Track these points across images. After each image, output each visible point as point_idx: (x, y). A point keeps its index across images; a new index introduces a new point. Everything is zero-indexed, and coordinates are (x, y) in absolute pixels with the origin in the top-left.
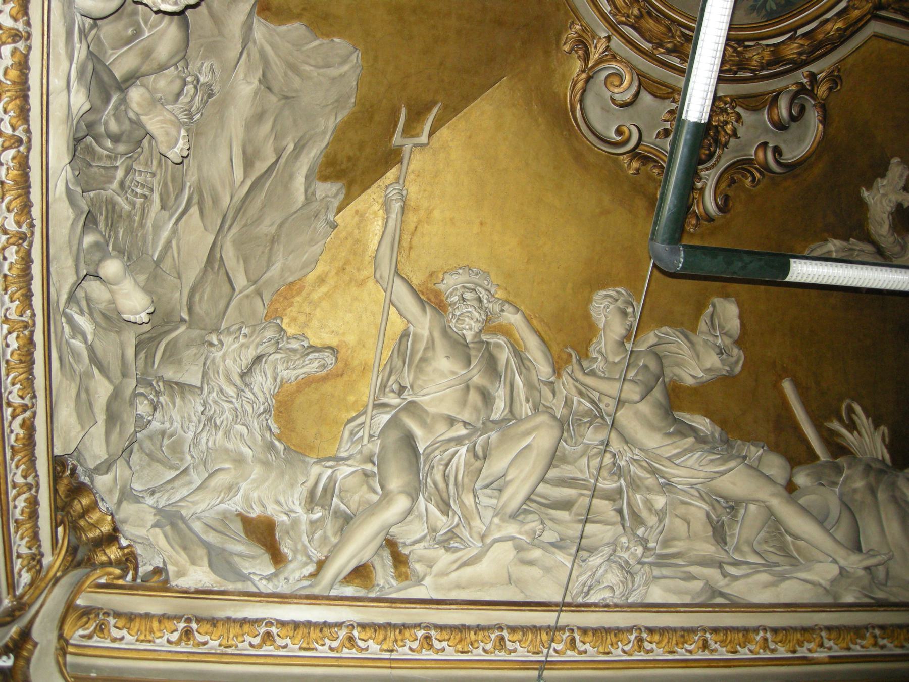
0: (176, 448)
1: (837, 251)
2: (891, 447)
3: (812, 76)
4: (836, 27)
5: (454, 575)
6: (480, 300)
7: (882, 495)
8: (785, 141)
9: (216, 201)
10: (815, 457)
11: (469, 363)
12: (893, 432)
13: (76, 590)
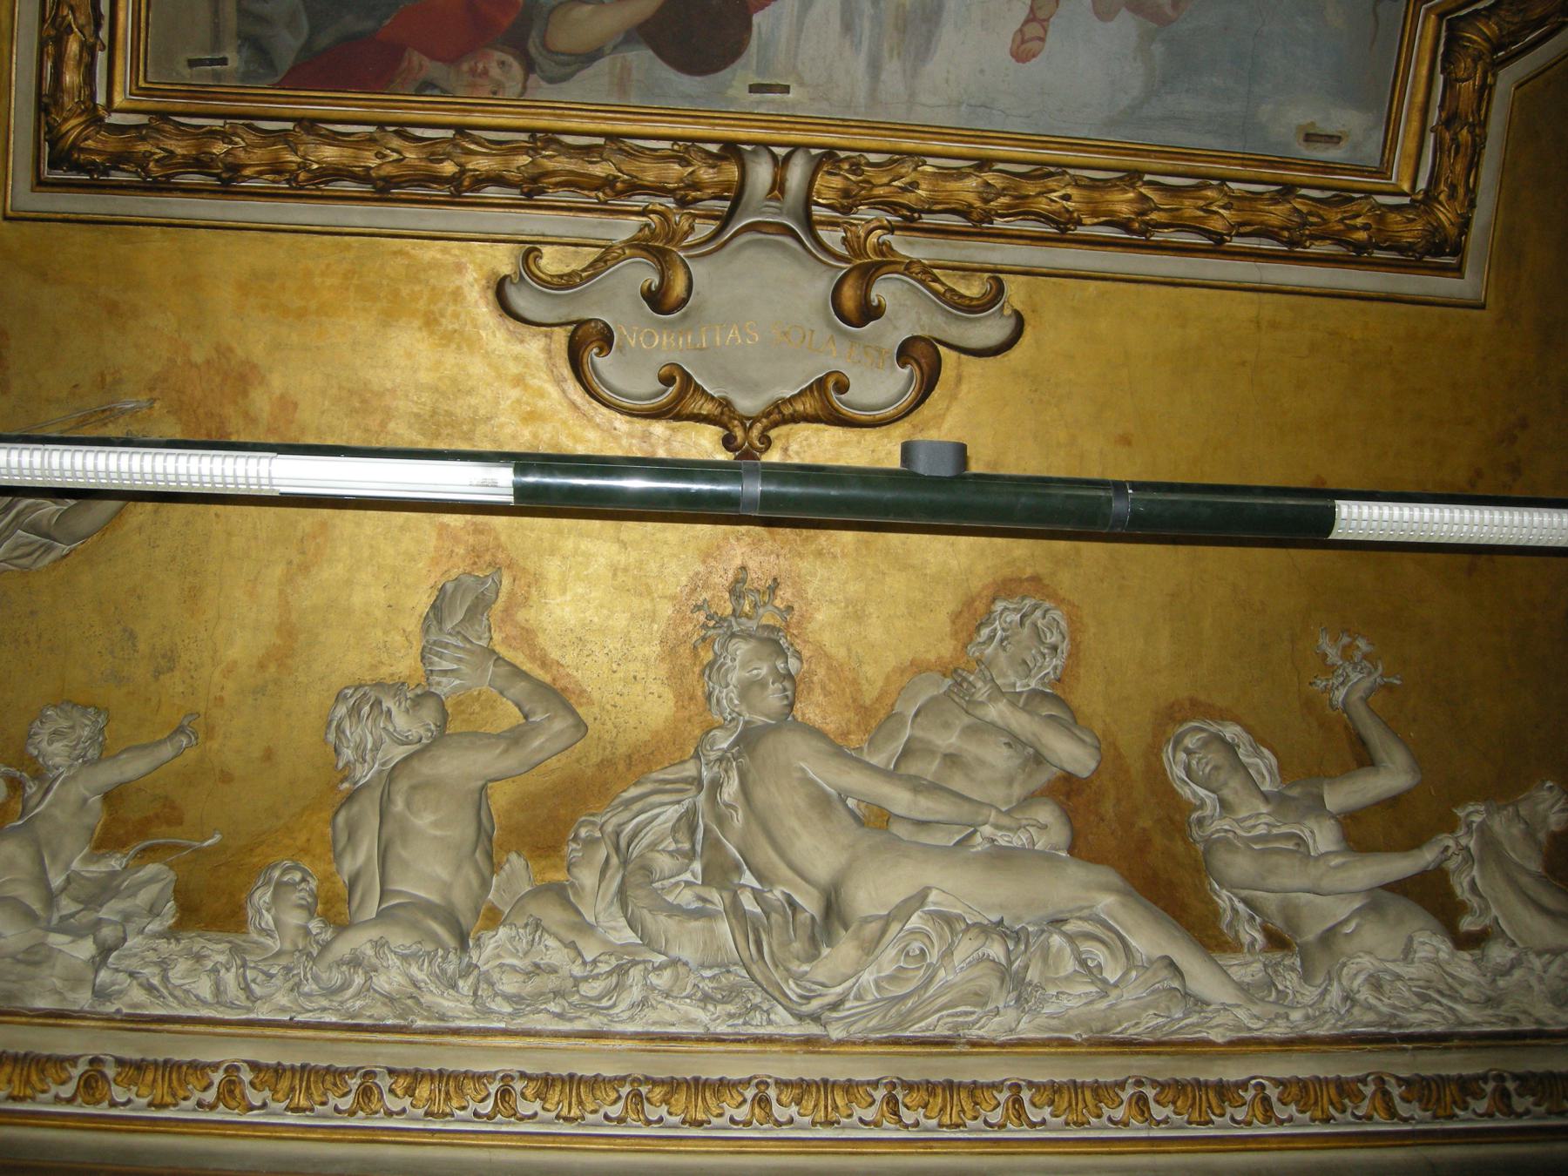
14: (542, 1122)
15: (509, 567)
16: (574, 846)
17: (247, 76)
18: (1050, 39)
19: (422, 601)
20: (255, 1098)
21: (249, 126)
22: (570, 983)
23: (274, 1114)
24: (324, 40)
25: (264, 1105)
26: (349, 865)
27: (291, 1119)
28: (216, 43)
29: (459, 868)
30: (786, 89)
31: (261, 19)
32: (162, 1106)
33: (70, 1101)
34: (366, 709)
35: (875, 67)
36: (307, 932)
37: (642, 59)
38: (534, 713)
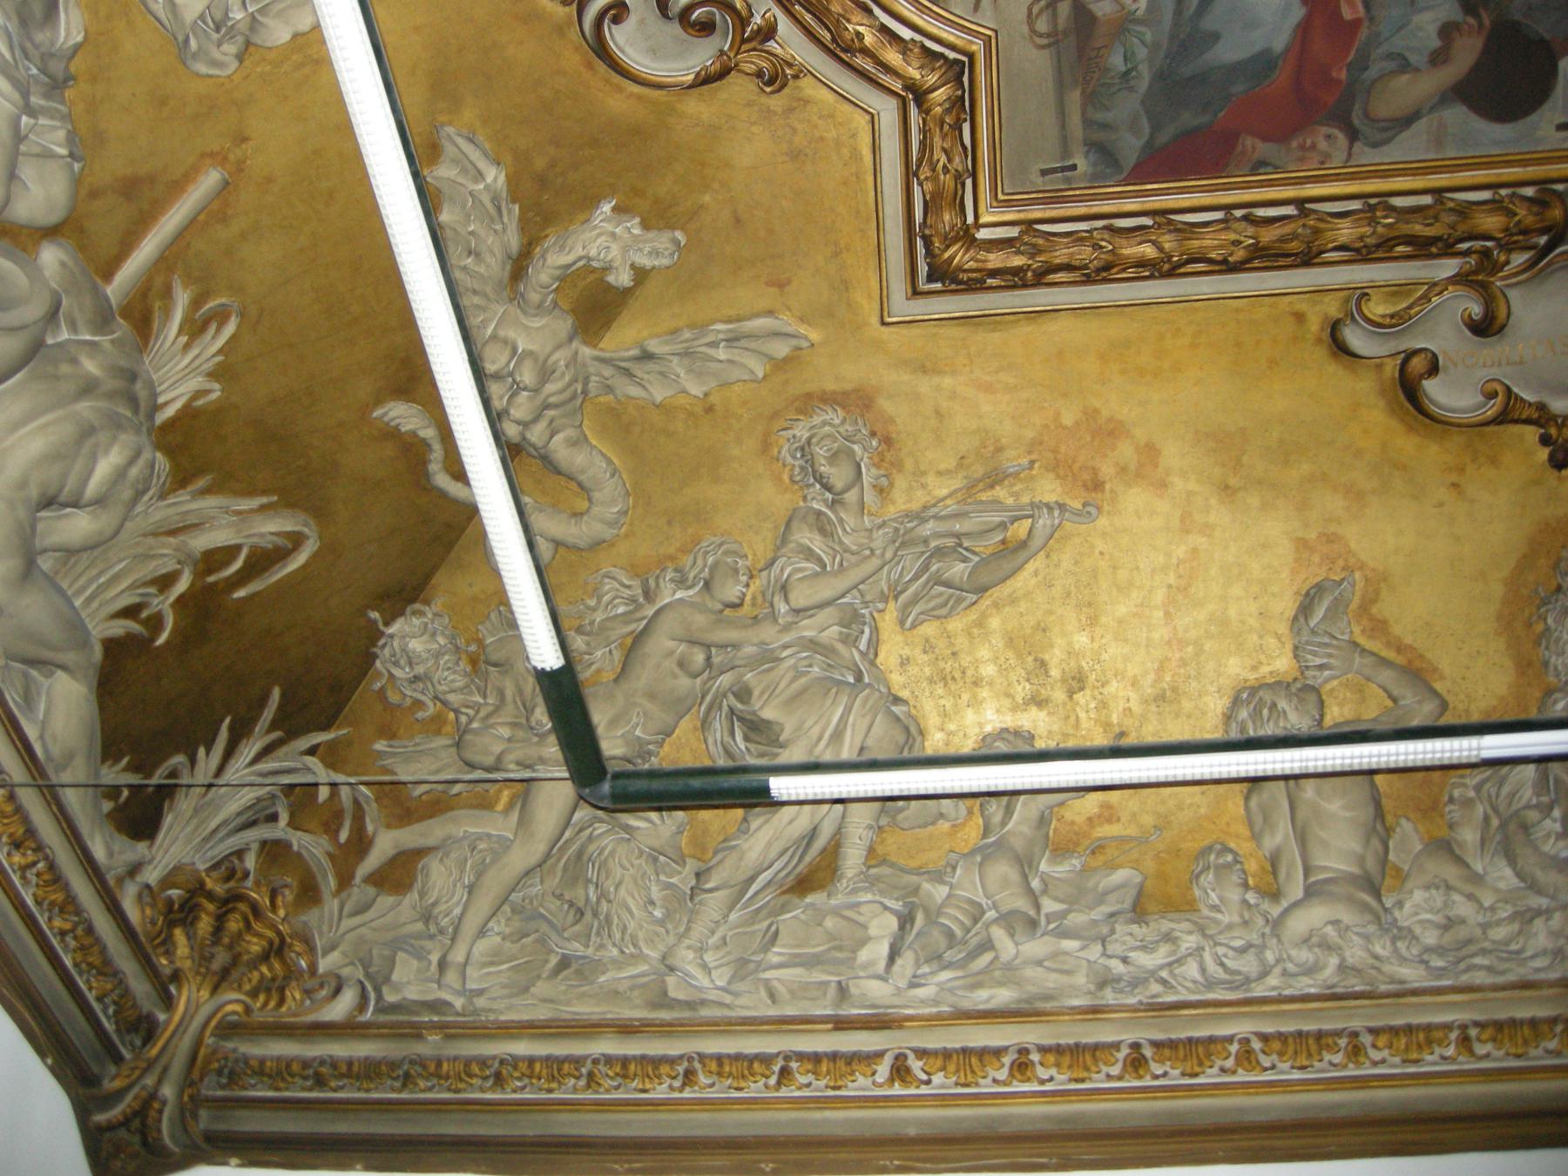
1: (487, 188)
2: (189, 413)
3: (769, 32)
4: (861, 29)
7: (84, 407)
8: (642, 22)
10: (108, 275)
12: (218, 413)
14: (1496, 1059)
15: (1361, 568)
16: (1452, 807)
17: (1095, 177)
19: (1286, 605)
20: (1266, 1061)
21: (1109, 228)
22: (1478, 932)
23: (1282, 1072)
24: (1164, 137)
25: (1273, 1067)
26: (1270, 843)
27: (1297, 1075)
28: (1066, 152)
29: (1368, 841)
31: (1105, 126)
32: (1196, 1075)
33: (1120, 1078)
34: (1265, 712)
36: (1245, 902)
37: (1457, 116)
38: (1404, 698)
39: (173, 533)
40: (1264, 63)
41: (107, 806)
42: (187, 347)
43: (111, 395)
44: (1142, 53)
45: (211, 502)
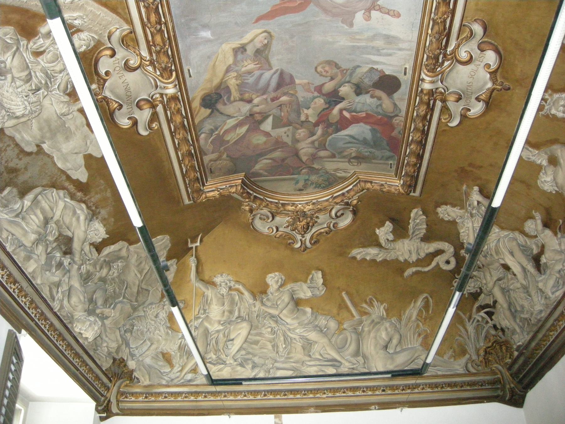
0: (142, 333)
5: (217, 373)
6: (226, 284)
7: (372, 335)
9: (134, 285)
11: (223, 304)
13: (119, 387)
18: (394, 9)
30: (406, 68)
35: (400, 49)
39: (409, 322)
40: (373, 131)
41: (452, 360)
42: (373, 307)
43: (373, 327)
44: (366, 150)
45: (407, 312)
